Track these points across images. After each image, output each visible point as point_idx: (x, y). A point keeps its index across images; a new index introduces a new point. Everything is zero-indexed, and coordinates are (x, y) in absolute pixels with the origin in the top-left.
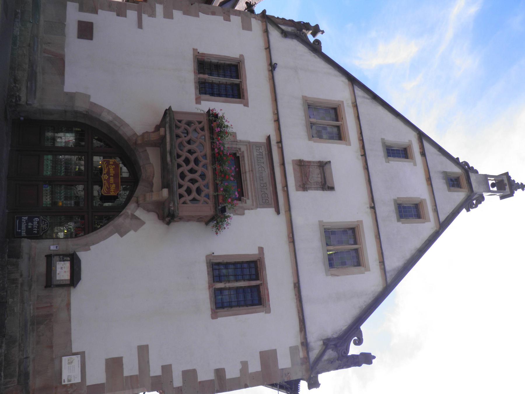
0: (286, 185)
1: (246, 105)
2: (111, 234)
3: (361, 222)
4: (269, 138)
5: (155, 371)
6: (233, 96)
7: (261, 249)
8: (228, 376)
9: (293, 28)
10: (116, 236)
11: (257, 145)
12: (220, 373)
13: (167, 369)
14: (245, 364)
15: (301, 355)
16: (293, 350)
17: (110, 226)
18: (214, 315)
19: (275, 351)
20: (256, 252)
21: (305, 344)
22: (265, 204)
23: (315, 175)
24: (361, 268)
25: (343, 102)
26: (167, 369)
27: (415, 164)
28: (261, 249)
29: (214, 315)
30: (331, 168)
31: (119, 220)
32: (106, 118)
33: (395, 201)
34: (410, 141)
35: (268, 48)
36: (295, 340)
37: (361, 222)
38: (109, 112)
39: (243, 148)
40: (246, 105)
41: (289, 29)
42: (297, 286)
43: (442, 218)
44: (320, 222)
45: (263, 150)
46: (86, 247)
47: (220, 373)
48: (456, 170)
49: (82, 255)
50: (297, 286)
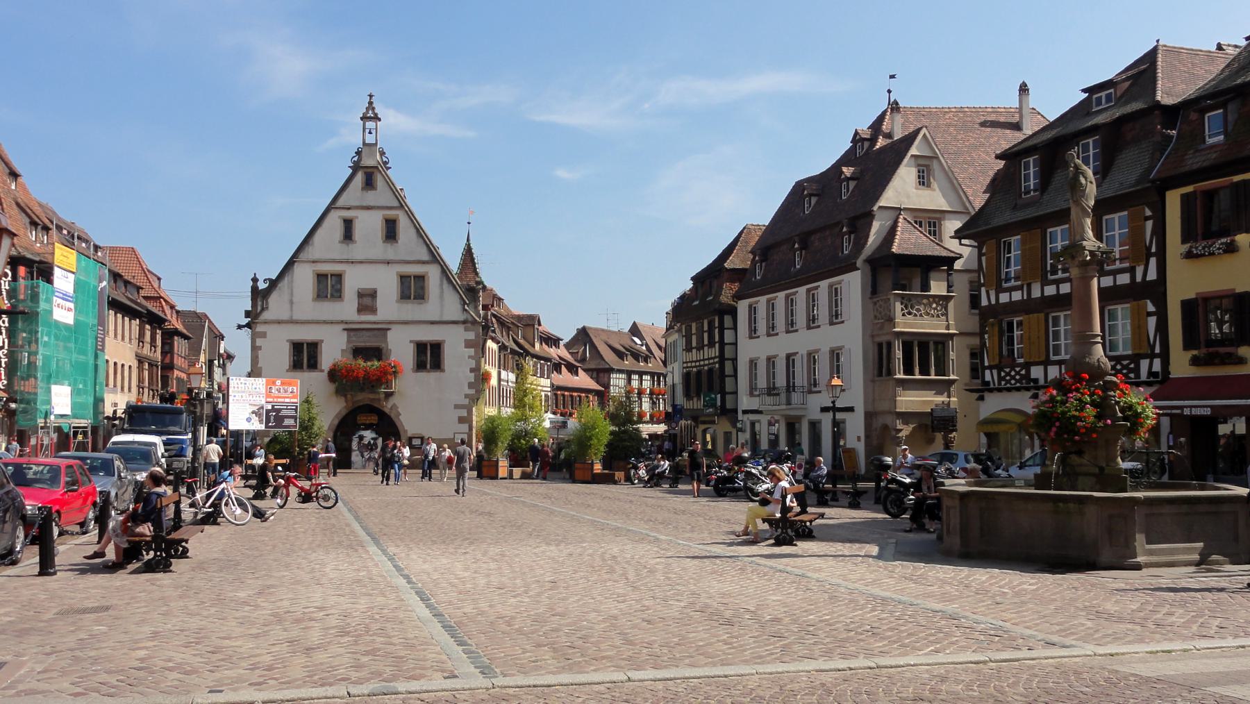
0: (375, 323)
1: (322, 341)
2: (399, 419)
3: (397, 272)
4: (344, 329)
5: (466, 402)
6: (317, 348)
7: (411, 342)
8: (474, 366)
9: (259, 300)
10: (400, 417)
11: (349, 337)
12: (472, 370)
13: (466, 396)
14: (469, 357)
15: (469, 325)
16: (466, 330)
17: (395, 420)
18: (443, 371)
19: (465, 340)
20: (412, 344)
21: (464, 322)
22: (385, 336)
23: (367, 301)
24: (426, 278)
25: (314, 271)
26: (466, 396)
27: (357, 217)
28: (411, 342)
29: (443, 371)
30: (362, 289)
31: (393, 416)
32: (336, 422)
33: (384, 242)
34: (339, 217)
35: (279, 322)
36: (461, 328)
37: (397, 272)
38: (333, 420)
39: (351, 345)
40: (322, 341)
41: (260, 303)
42: (433, 323)
43: (396, 204)
44: (397, 302)
45: (352, 334)
46: (406, 431)
47: (472, 370)
48: (360, 177)
49: (410, 434)
50: (433, 323)
